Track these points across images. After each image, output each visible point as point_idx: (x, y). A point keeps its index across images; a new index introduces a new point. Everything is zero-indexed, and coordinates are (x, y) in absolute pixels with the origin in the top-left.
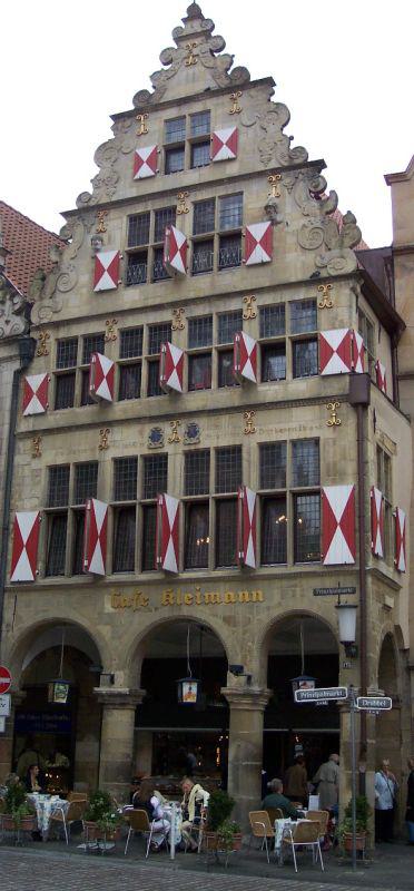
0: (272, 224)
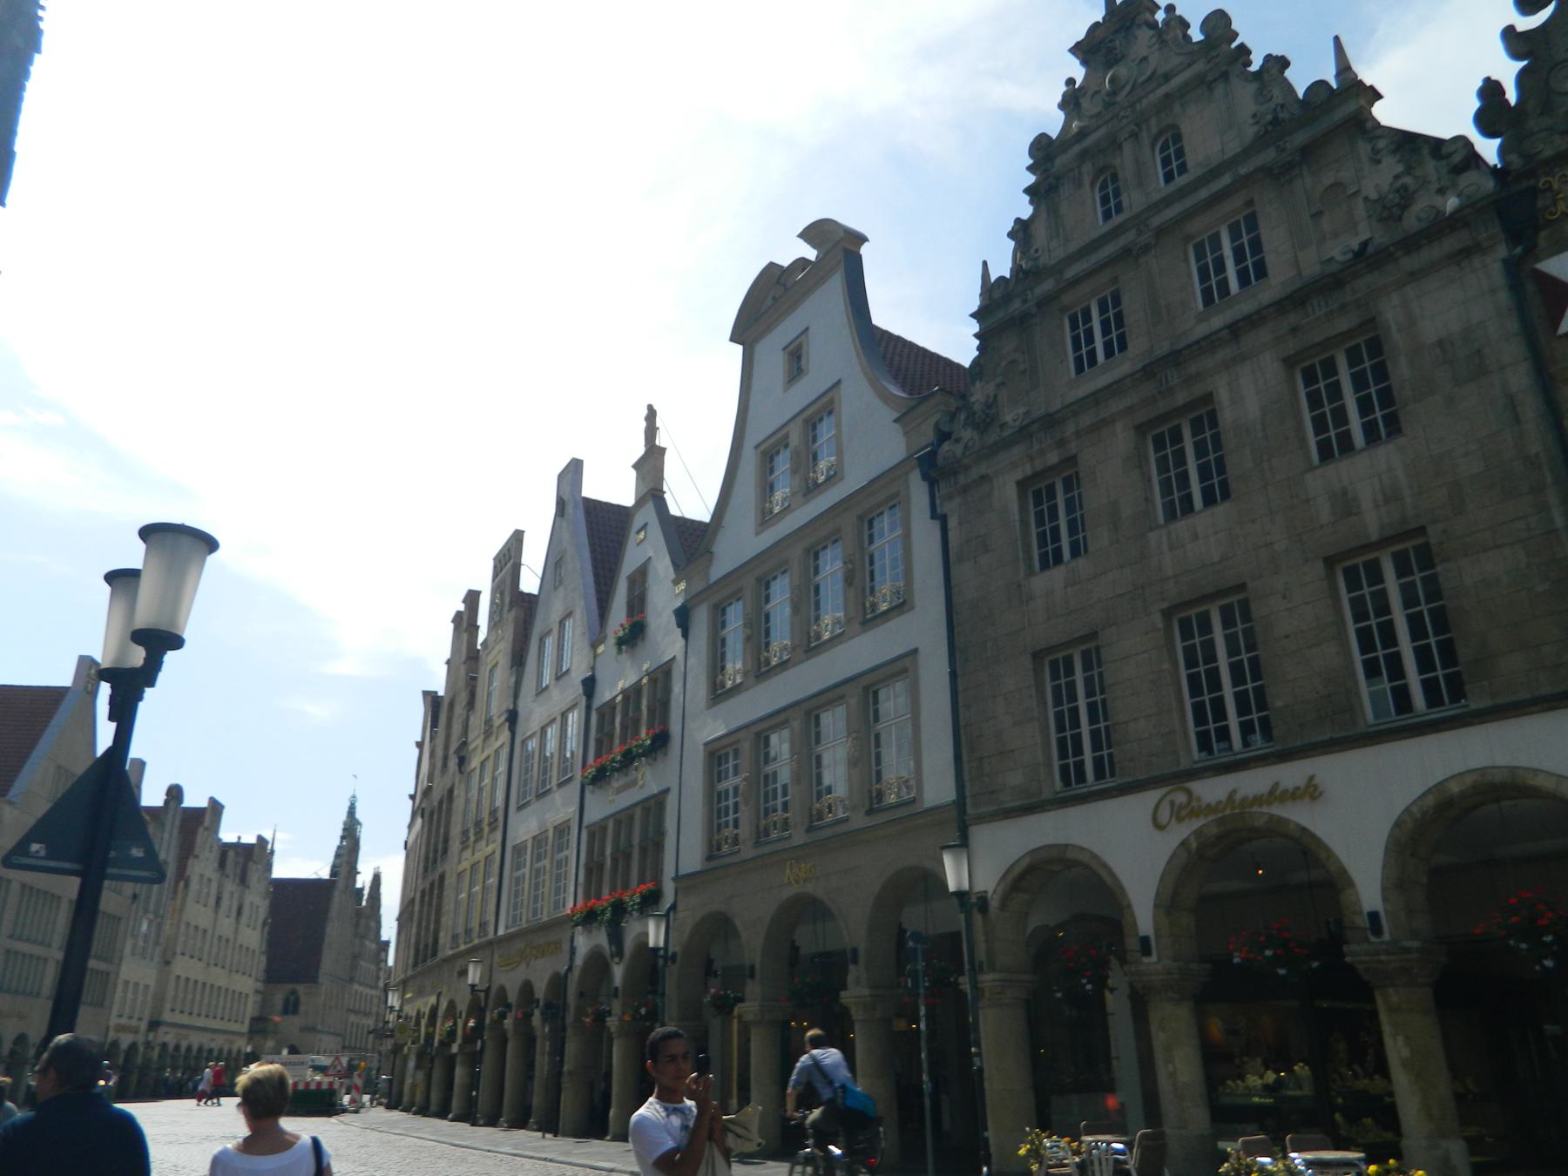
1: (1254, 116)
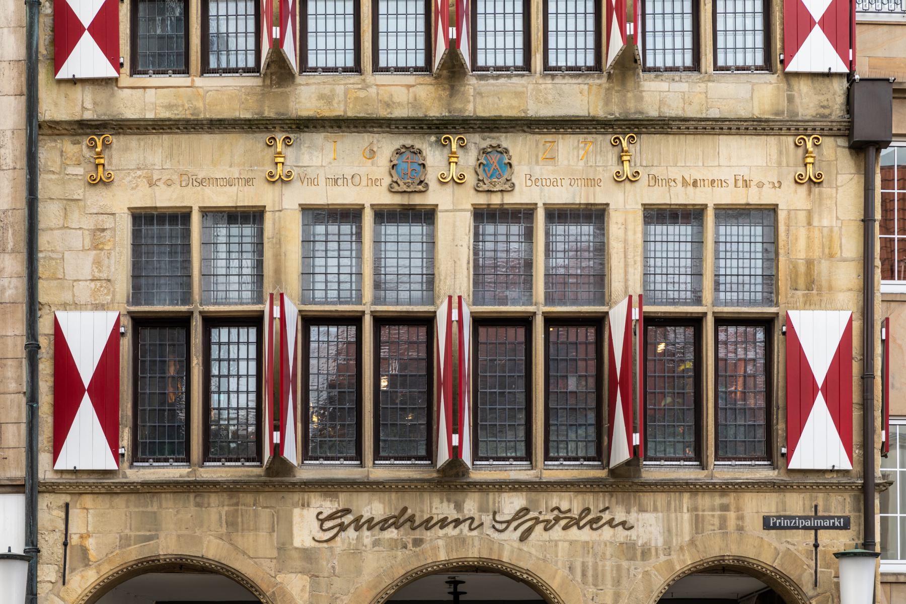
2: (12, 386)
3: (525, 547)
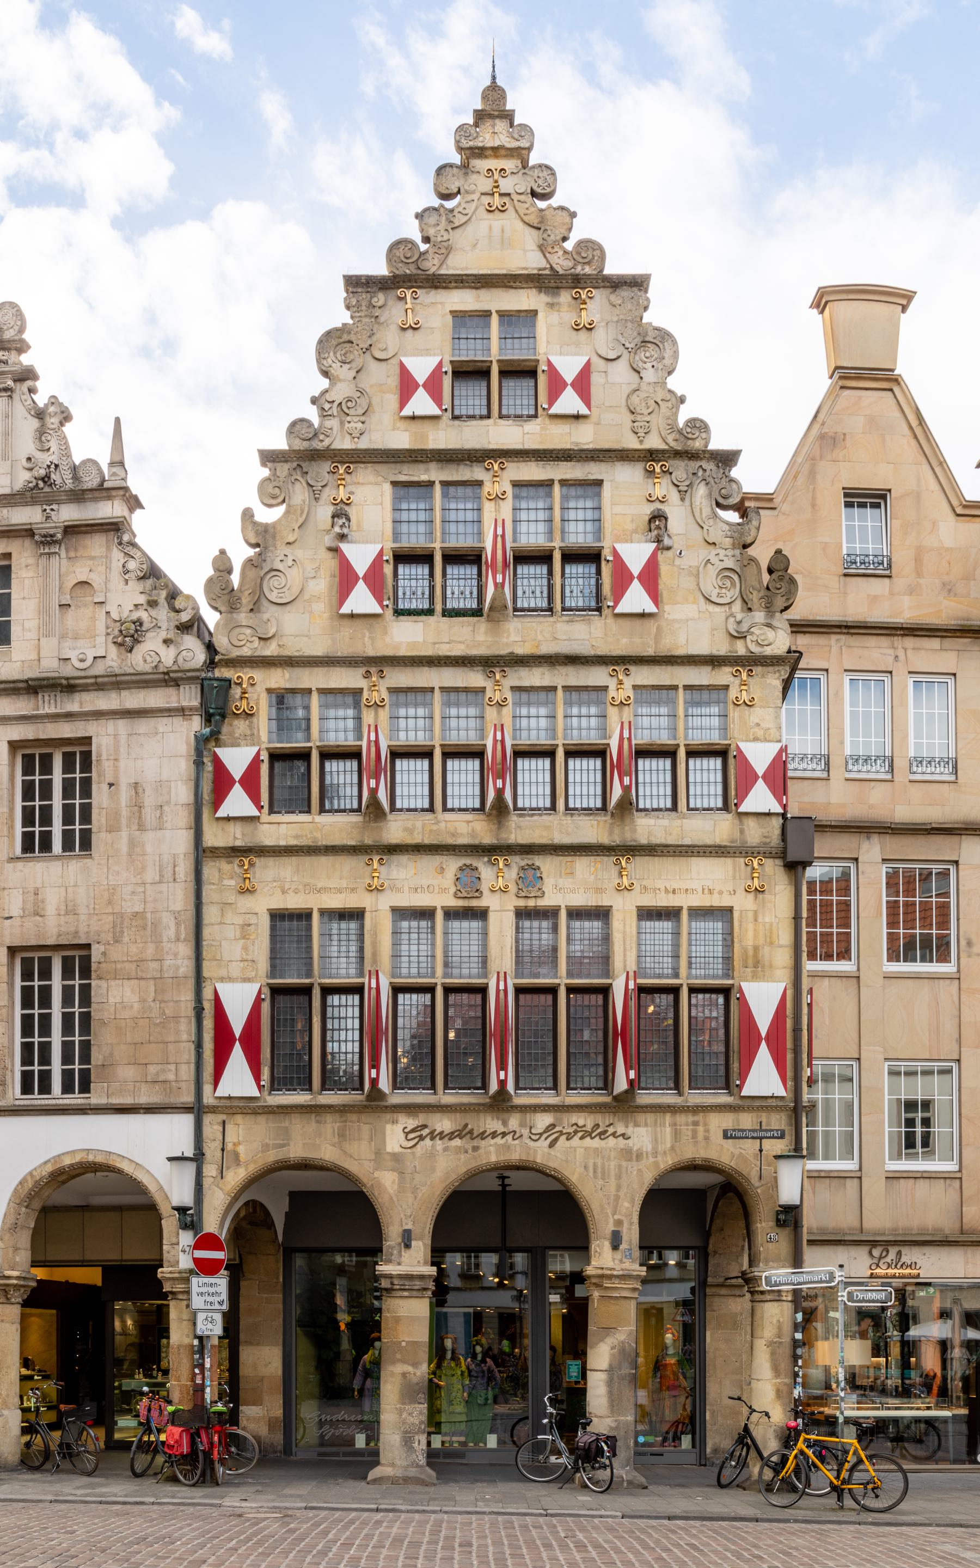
0: (657, 549)
1: (29, 459)
2: (185, 1037)
3: (552, 1151)
